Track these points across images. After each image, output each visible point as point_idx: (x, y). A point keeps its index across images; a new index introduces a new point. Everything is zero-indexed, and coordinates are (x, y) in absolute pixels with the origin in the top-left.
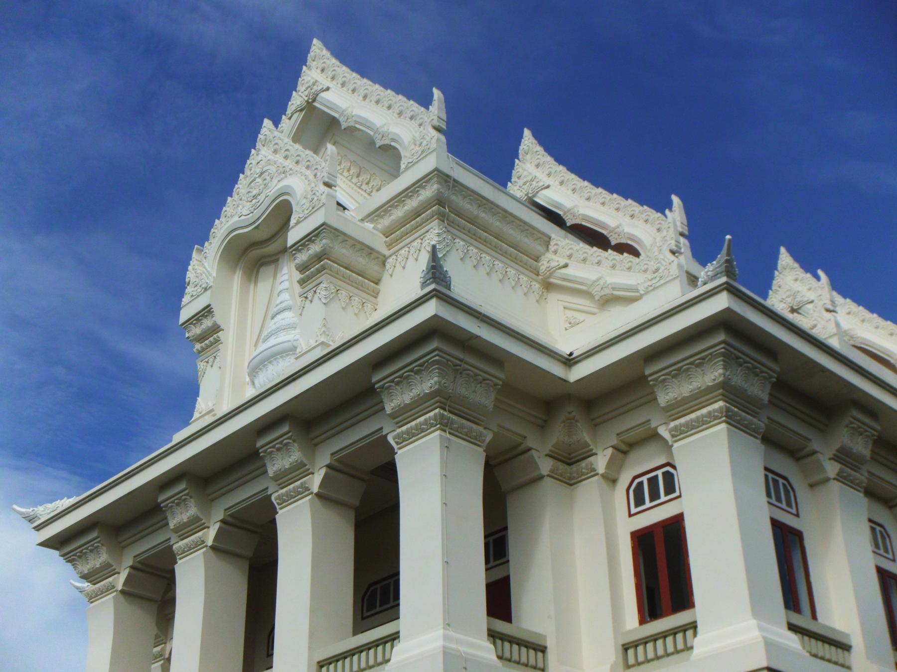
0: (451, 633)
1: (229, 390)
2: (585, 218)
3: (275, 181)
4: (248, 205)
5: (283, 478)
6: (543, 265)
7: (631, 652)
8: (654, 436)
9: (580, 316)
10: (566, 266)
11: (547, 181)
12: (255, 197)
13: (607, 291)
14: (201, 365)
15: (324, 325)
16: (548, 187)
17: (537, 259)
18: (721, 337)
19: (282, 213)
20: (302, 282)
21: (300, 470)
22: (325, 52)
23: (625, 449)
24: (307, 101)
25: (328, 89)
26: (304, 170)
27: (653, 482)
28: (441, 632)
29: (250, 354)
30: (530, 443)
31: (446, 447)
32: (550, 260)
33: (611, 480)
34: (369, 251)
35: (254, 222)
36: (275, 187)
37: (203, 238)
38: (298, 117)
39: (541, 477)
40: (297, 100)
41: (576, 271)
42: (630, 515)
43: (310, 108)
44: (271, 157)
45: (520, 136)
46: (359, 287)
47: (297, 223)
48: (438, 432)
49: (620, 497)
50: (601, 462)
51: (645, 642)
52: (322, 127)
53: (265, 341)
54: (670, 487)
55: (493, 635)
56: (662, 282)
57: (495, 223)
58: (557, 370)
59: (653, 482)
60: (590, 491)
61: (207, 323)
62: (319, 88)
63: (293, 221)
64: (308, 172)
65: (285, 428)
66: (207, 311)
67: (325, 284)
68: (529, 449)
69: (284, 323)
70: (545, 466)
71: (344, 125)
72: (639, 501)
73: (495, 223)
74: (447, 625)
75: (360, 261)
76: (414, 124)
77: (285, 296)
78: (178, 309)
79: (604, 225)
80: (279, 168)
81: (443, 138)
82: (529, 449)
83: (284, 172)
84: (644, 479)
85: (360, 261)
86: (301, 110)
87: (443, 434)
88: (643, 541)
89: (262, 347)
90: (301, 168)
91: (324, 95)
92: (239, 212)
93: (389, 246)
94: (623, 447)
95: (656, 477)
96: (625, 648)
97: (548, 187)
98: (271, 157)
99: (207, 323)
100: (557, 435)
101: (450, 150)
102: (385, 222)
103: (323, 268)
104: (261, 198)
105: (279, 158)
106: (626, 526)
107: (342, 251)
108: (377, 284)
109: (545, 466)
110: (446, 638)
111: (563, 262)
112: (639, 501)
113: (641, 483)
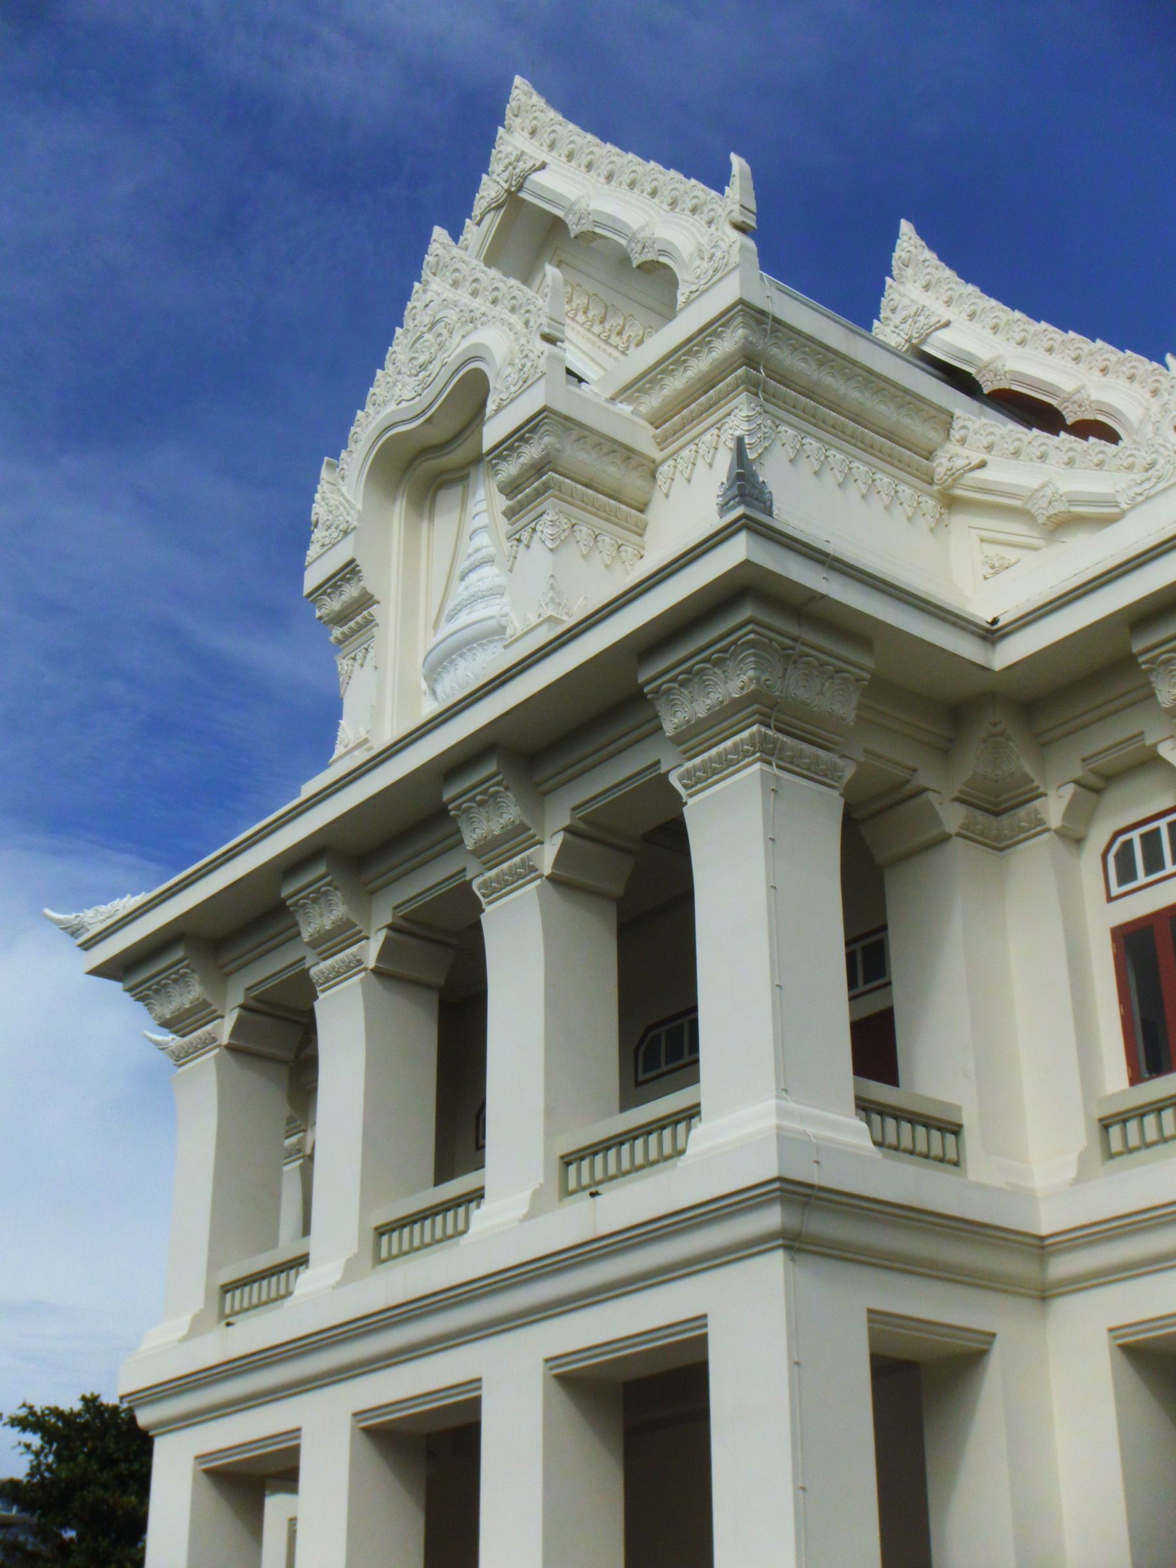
0: (791, 1105)
1: (392, 705)
2: (1017, 377)
3: (456, 337)
4: (413, 381)
5: (491, 851)
6: (941, 465)
7: (1115, 1131)
8: (1151, 761)
9: (1011, 554)
10: (982, 465)
11: (946, 314)
12: (423, 367)
13: (1061, 507)
14: (343, 665)
15: (552, 588)
16: (947, 324)
17: (929, 455)
19: (471, 393)
20: (510, 514)
21: (519, 837)
22: (537, 99)
23: (1098, 785)
24: (508, 191)
25: (543, 166)
26: (506, 315)
28: (772, 1102)
29: (426, 642)
30: (922, 779)
31: (773, 791)
32: (952, 457)
33: (1074, 839)
34: (626, 454)
35: (423, 412)
36: (457, 347)
37: (336, 443)
38: (493, 221)
39: (945, 838)
40: (490, 189)
41: (1000, 473)
42: (1110, 899)
43: (513, 202)
44: (449, 294)
45: (894, 235)
46: (611, 517)
47: (498, 410)
48: (758, 766)
49: (1089, 867)
50: (1054, 807)
51: (1140, 1113)
52: (538, 236)
53: (451, 618)
55: (865, 1107)
56: (1162, 485)
57: (853, 394)
58: (967, 648)
59: (1151, 841)
60: (1035, 860)
61: (350, 592)
62: (528, 166)
63: (491, 407)
64: (514, 319)
65: (491, 767)
66: (350, 571)
67: (551, 511)
68: (924, 790)
69: (482, 586)
70: (952, 817)
71: (574, 230)
73: (853, 394)
74: (784, 1091)
75: (612, 472)
76: (700, 220)
77: (483, 539)
78: (300, 569)
79: (1053, 391)
80: (464, 314)
81: (751, 244)
82: (924, 790)
83: (473, 320)
84: (1135, 835)
85: (612, 472)
86: (499, 207)
87: (766, 767)
89: (446, 629)
90: (502, 311)
91: (536, 177)
92: (398, 394)
93: (662, 443)
94: (1095, 782)
95: (1157, 831)
96: (1105, 1125)
97: (947, 324)
98: (449, 294)
99: (350, 592)
100: (972, 764)
101: (764, 266)
102: (653, 401)
103: (547, 487)
104: (434, 368)
105: (462, 296)
106: (1103, 916)
107: (578, 456)
108: (642, 511)
109: (952, 817)
110: (781, 1112)
111: (976, 458)
112: (1126, 872)
113: (1129, 844)
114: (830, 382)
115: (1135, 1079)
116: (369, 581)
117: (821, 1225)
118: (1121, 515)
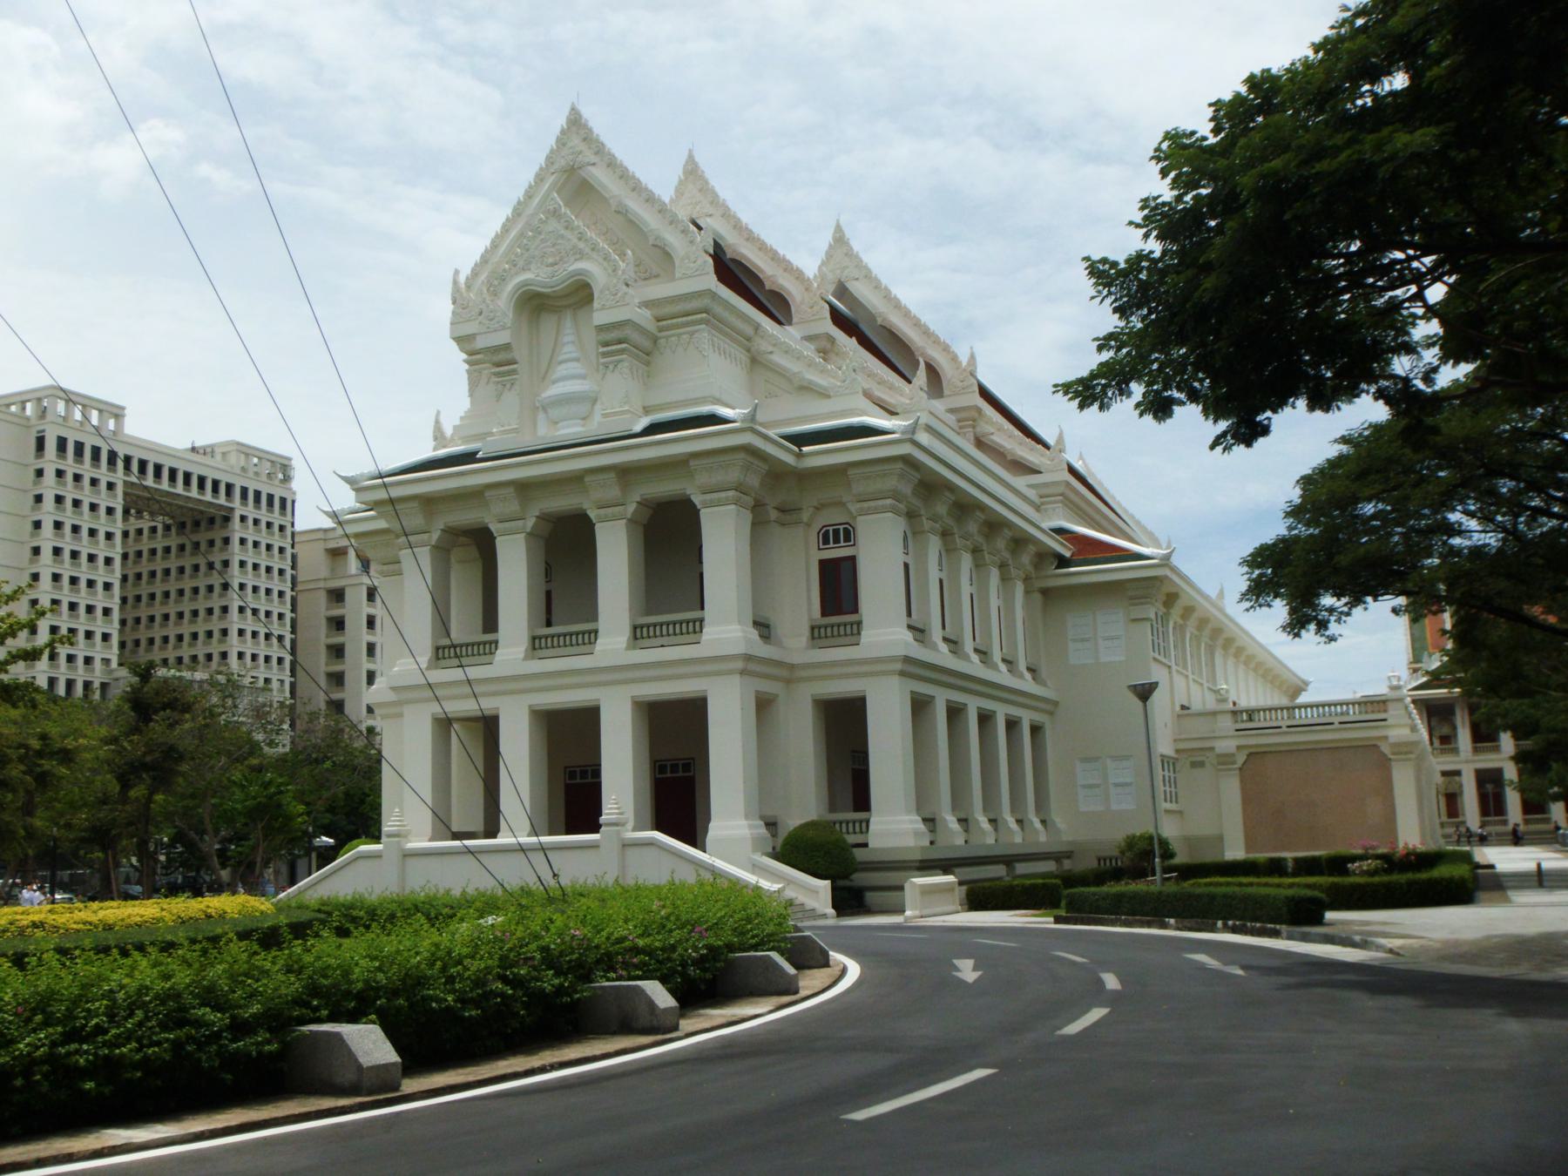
8: (842, 504)
18: (900, 465)
27: (836, 532)
33: (808, 525)
39: (768, 522)
41: (778, 358)
50: (805, 516)
54: (847, 539)
59: (836, 532)
70: (774, 514)
72: (826, 541)
81: (710, 261)
88: (823, 564)
90: (594, 255)
105: (568, 234)
106: (817, 555)
114: (726, 315)
115: (824, 614)
116: (516, 355)
117: (752, 666)
118: (829, 397)
